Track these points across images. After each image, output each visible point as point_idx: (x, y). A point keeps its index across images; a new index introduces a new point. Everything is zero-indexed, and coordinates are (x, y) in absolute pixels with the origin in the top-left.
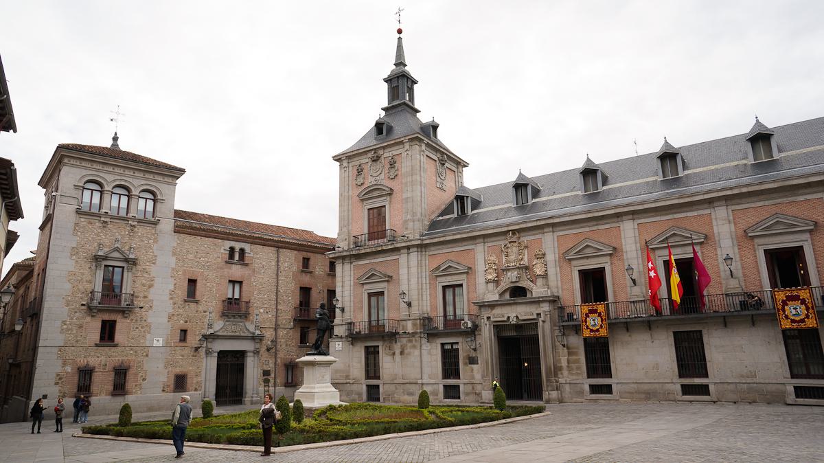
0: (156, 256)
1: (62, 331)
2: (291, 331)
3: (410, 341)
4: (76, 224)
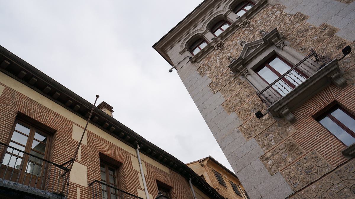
0: (298, 13)
1: (272, 172)
4: (199, 69)
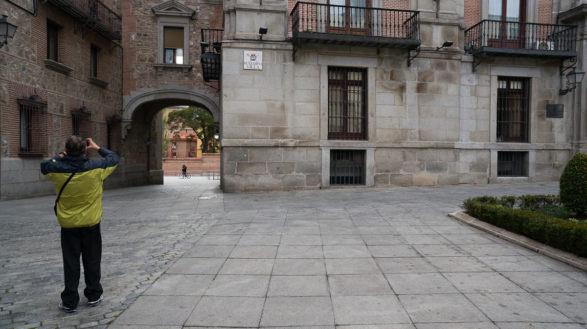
2: (29, 19)
3: (440, 66)
